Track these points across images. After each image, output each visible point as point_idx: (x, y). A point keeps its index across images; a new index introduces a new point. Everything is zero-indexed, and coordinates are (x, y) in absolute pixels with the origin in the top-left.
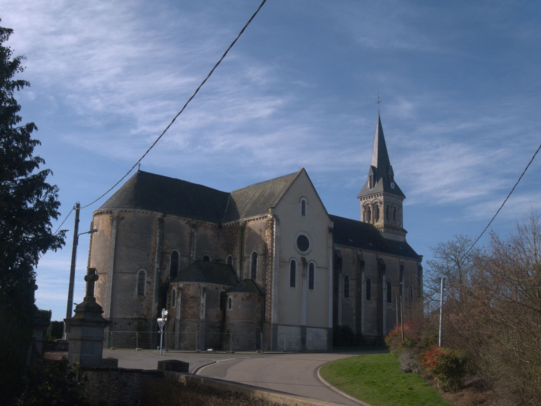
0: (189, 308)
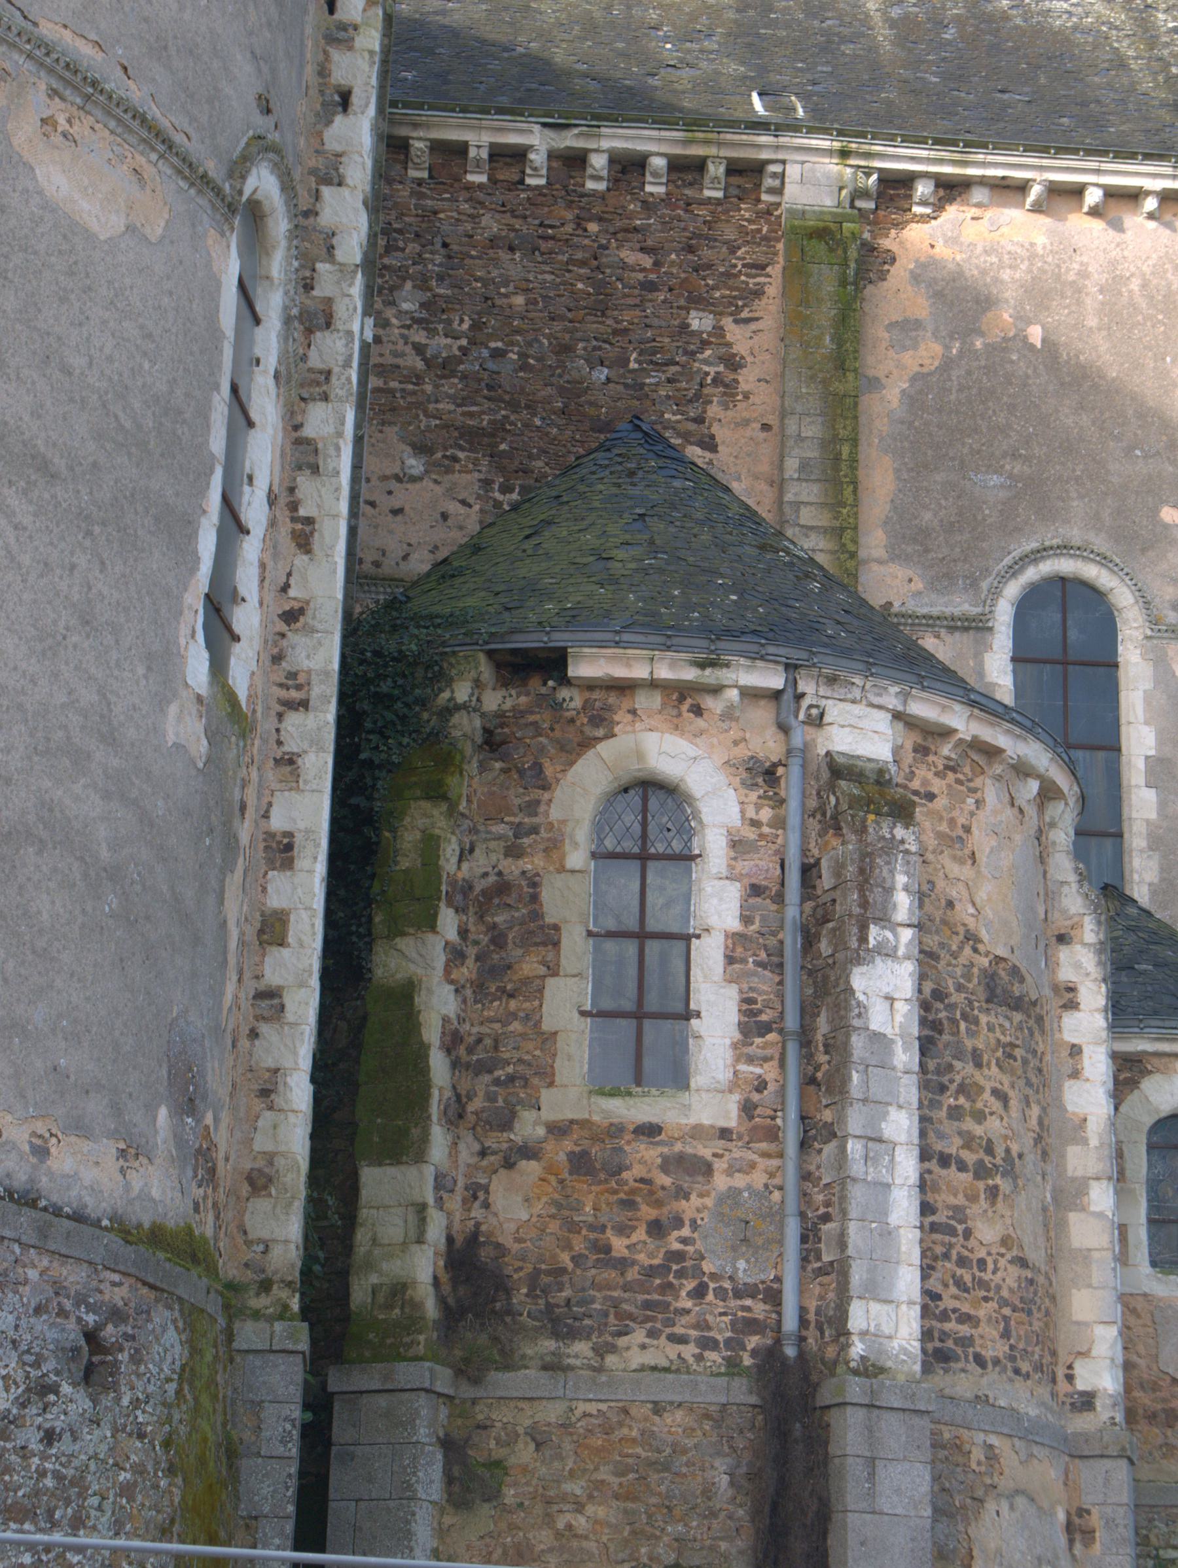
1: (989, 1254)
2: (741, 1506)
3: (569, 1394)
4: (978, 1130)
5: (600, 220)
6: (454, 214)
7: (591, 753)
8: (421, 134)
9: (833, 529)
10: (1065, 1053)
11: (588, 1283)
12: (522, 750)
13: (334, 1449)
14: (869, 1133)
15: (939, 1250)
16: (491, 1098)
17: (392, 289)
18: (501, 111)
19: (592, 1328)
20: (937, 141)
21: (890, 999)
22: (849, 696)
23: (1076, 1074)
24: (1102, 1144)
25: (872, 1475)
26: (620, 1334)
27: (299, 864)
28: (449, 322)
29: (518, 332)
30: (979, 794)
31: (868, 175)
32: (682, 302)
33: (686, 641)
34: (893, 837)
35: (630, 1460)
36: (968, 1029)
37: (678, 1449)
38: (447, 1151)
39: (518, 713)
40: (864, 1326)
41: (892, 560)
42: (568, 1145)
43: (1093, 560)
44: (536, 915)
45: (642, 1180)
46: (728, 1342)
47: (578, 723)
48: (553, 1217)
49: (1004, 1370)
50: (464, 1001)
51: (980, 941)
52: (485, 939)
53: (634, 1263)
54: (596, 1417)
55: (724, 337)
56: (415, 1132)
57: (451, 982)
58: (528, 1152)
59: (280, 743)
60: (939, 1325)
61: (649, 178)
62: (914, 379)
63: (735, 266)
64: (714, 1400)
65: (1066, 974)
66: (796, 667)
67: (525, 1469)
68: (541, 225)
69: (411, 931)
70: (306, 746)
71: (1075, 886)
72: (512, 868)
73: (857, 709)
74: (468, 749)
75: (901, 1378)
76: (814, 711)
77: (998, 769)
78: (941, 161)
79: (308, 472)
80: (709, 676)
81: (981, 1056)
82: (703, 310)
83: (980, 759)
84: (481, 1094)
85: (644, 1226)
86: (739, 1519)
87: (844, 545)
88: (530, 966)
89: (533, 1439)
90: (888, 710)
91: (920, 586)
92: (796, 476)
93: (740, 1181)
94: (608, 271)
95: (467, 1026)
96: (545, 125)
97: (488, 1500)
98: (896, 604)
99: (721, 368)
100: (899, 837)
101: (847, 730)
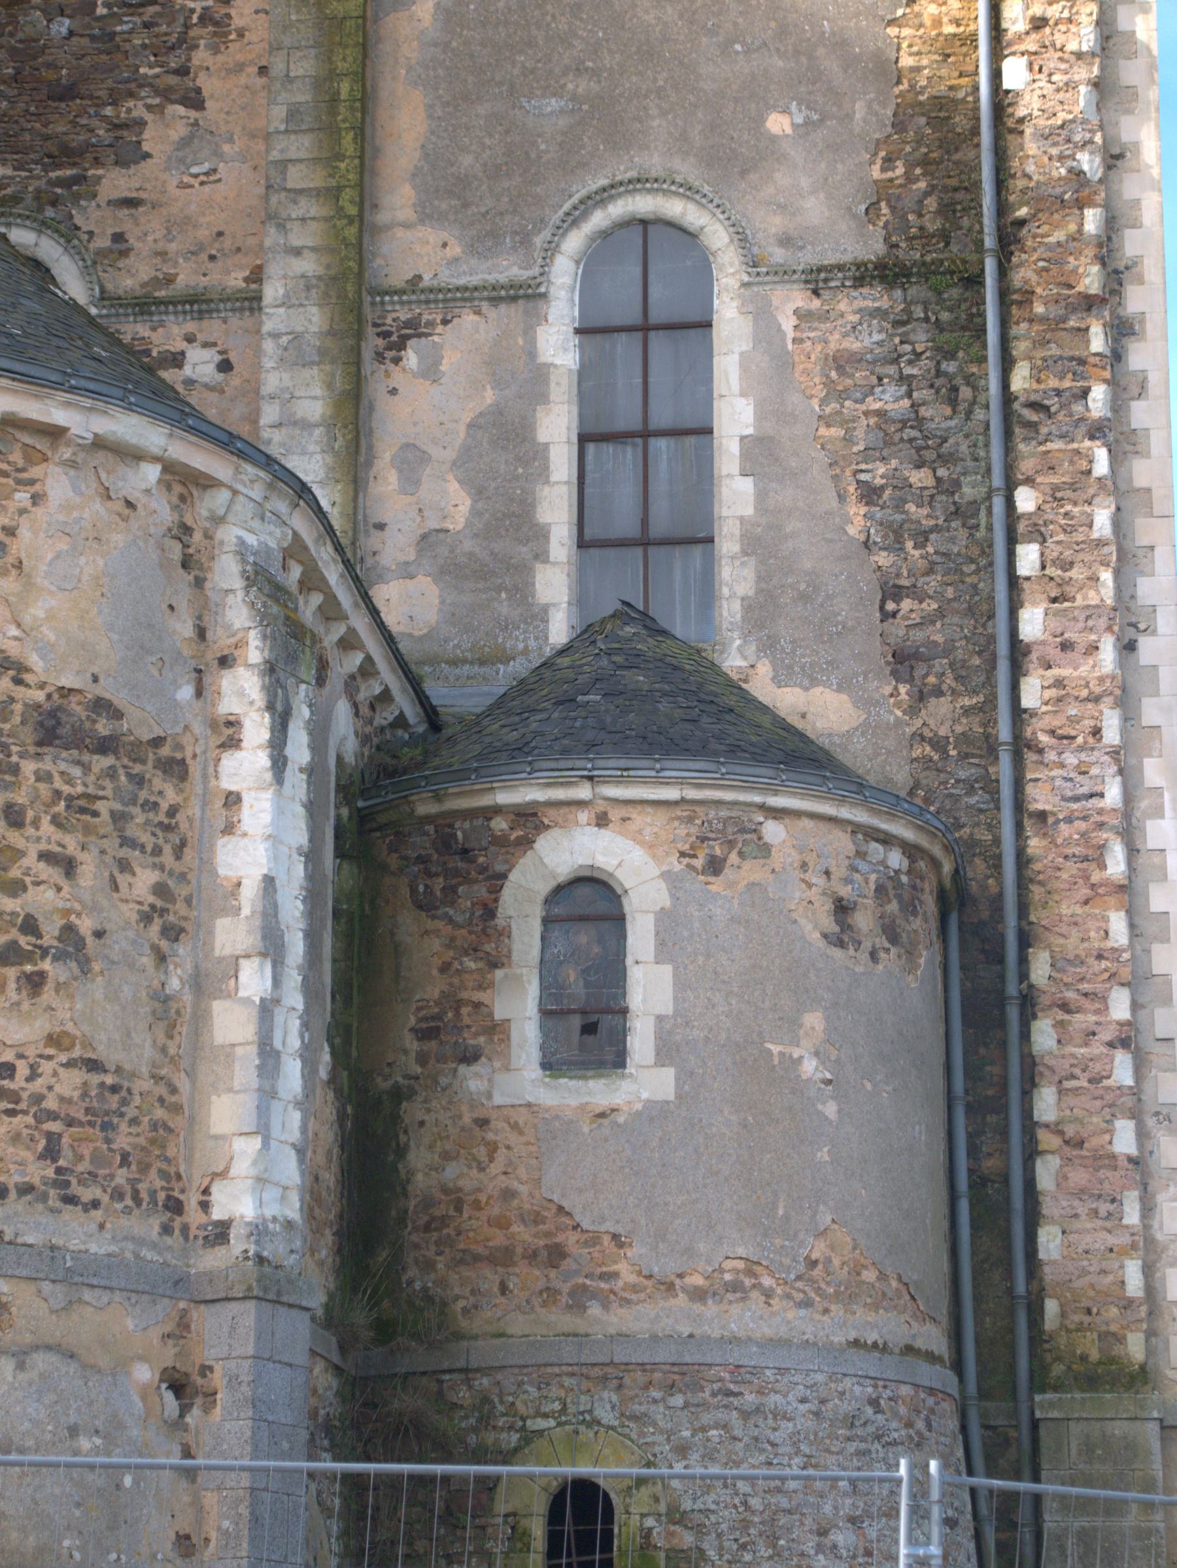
1: (21, 1056)
9: (328, 189)
10: (219, 803)
23: (229, 829)
24: (253, 912)
30: (37, 487)
41: (422, 221)
43: (676, 194)
49: (44, 1197)
51: (28, 670)
65: (228, 705)
71: (240, 594)
81: (22, 812)
83: (41, 444)
87: (342, 208)
91: (458, 250)
92: (282, 127)
98: (427, 277)
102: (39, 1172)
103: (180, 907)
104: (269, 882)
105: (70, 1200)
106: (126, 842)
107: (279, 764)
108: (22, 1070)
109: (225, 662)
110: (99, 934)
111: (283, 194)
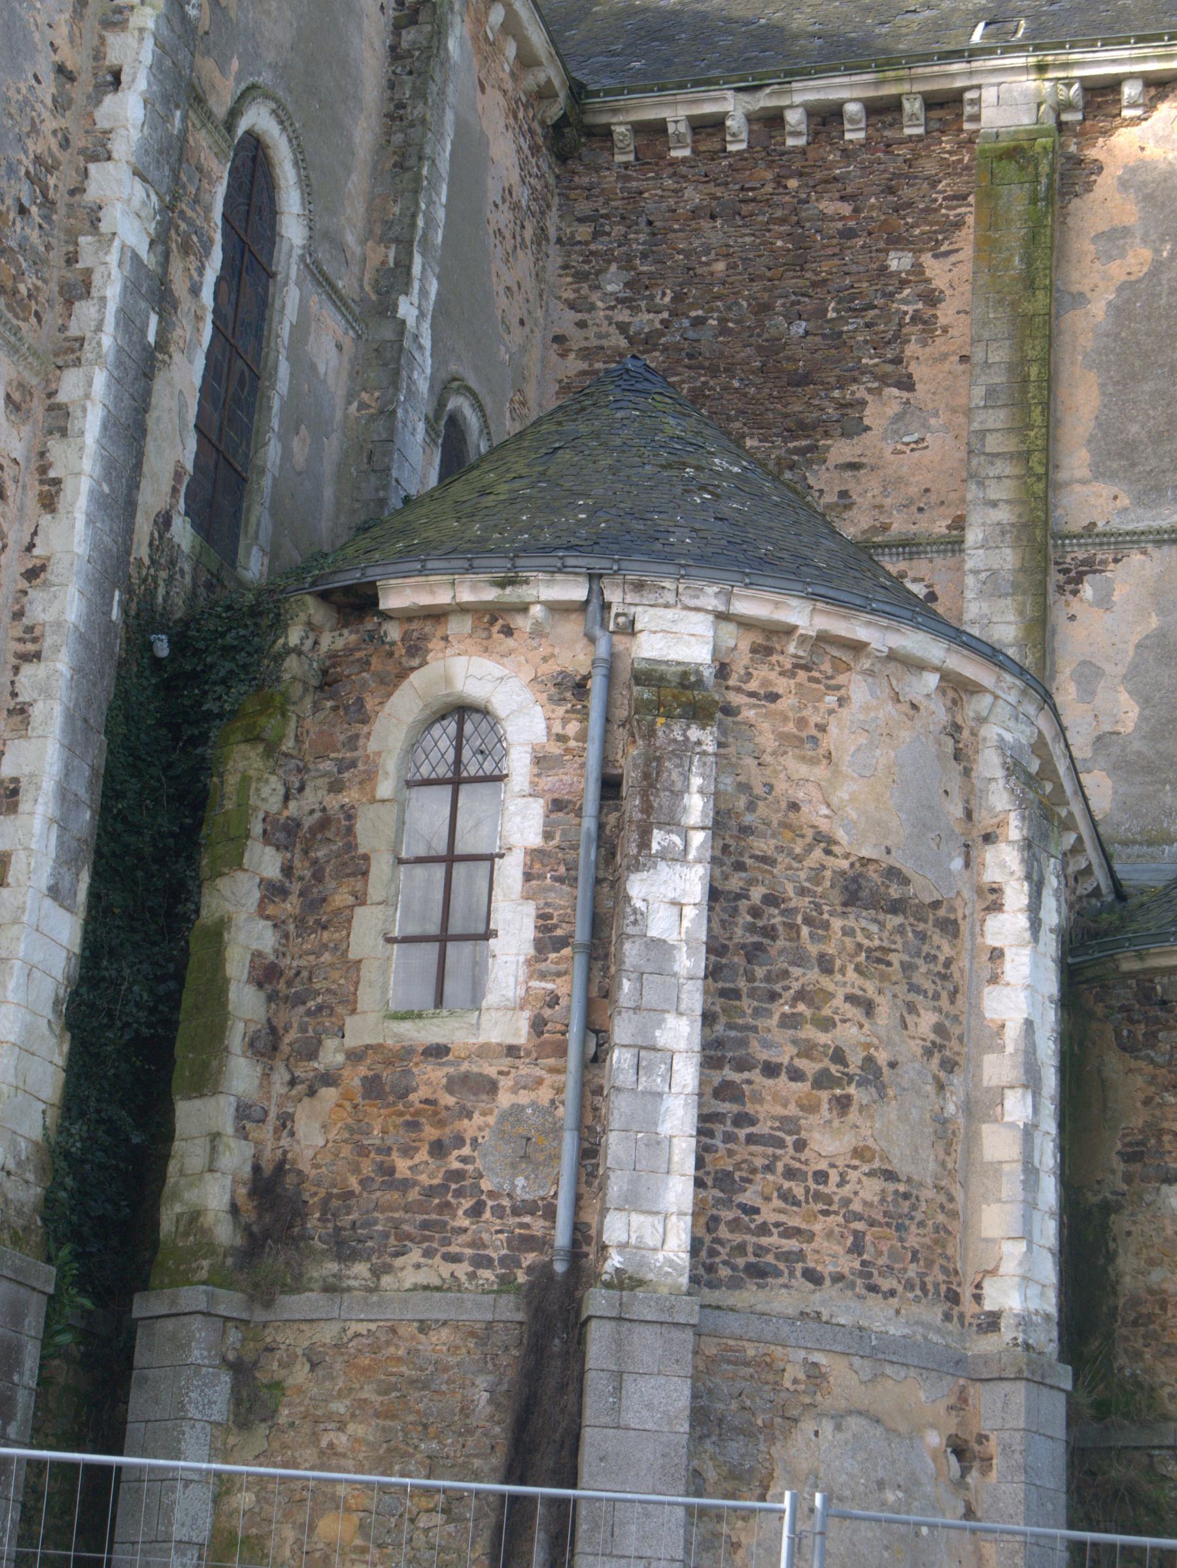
0: (823, 1080)
1: (832, 1166)
2: (499, 1423)
3: (344, 1315)
4: (822, 1038)
5: (801, 175)
6: (659, 192)
7: (405, 683)
8: (622, 118)
9: (1020, 453)
10: (985, 957)
11: (372, 1205)
12: (348, 687)
13: (135, 1373)
14: (640, 1042)
15: (759, 1162)
16: (303, 1029)
17: (598, 273)
18: (696, 83)
19: (372, 1249)
20: (1140, 39)
21: (678, 905)
22: (660, 601)
23: (994, 979)
24: (1016, 1050)
25: (618, 1389)
26: (397, 1254)
27: (24, 807)
28: (652, 297)
29: (718, 297)
30: (843, 692)
31: (1069, 86)
32: (882, 245)
33: (485, 562)
34: (687, 739)
35: (393, 1379)
36: (811, 935)
37: (440, 1367)
38: (257, 1082)
39: (349, 650)
40: (623, 1238)
41: (1096, 478)
42: (362, 1070)
44: (351, 846)
45: (427, 1101)
46: (503, 1260)
47: (397, 655)
48: (345, 1141)
49: (852, 1286)
50: (286, 936)
51: (836, 843)
52: (308, 874)
53: (415, 1183)
54: (368, 1336)
55: (923, 273)
56: (215, 1063)
57: (268, 918)
58: (329, 1079)
59: (14, 695)
60: (754, 1239)
61: (847, 126)
62: (1120, 289)
63: (936, 200)
64: (479, 1317)
65: (991, 875)
66: (601, 576)
67: (300, 1390)
68: (742, 189)
69: (226, 870)
70: (35, 695)
71: (1001, 782)
72: (333, 802)
73: (670, 614)
74: (297, 691)
75: (664, 1291)
76: (621, 620)
77: (866, 664)
78: (1145, 59)
79: (58, 435)
80: (511, 594)
81: (831, 962)
82: (902, 250)
83: (846, 656)
84: (295, 1025)
85: (427, 1147)
86: (495, 1437)
87: (1032, 468)
88: (341, 898)
89: (309, 1360)
90: (707, 611)
91: (1127, 502)
92: (982, 404)
93: (524, 1098)
94: (808, 225)
95: (288, 961)
96: (738, 90)
97: (264, 1420)
98: (1100, 524)
99: (920, 306)
100: (693, 739)
101: (659, 635)
102: (848, 1264)
103: (954, 1043)
104: (1029, 1024)
105: (873, 1288)
106: (913, 988)
107: (1035, 924)
108: (834, 1177)
109: (988, 839)
110: (893, 1065)
111: (983, 458)
